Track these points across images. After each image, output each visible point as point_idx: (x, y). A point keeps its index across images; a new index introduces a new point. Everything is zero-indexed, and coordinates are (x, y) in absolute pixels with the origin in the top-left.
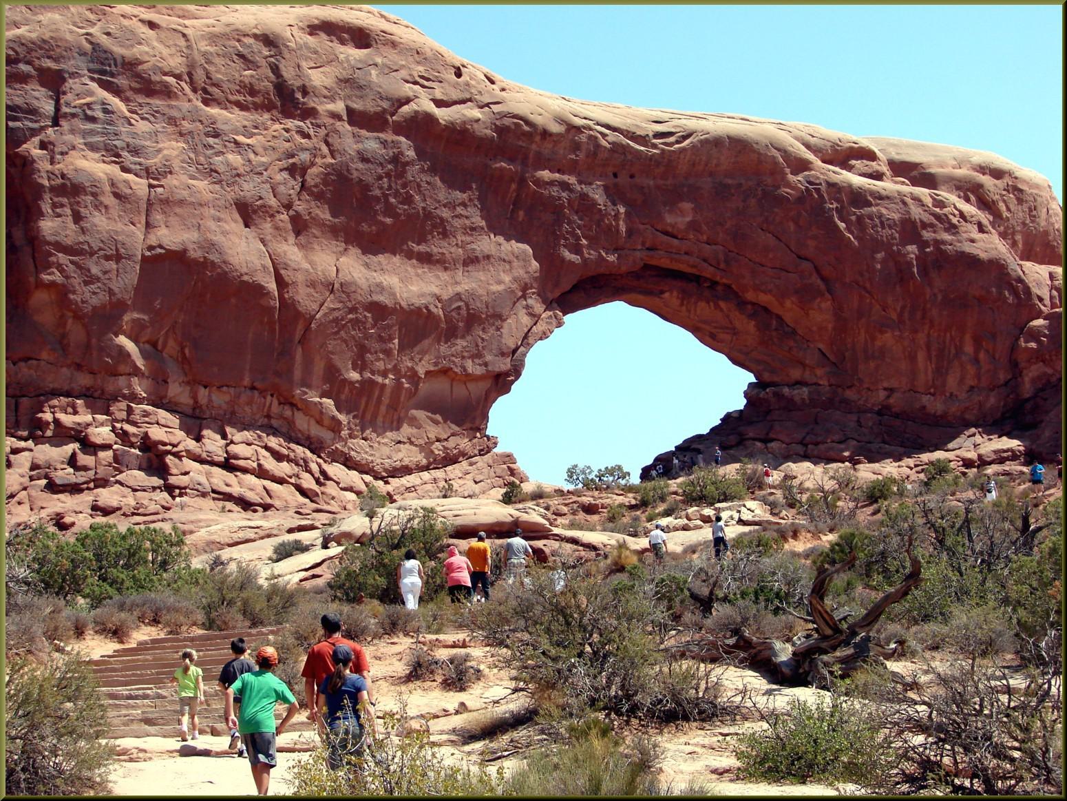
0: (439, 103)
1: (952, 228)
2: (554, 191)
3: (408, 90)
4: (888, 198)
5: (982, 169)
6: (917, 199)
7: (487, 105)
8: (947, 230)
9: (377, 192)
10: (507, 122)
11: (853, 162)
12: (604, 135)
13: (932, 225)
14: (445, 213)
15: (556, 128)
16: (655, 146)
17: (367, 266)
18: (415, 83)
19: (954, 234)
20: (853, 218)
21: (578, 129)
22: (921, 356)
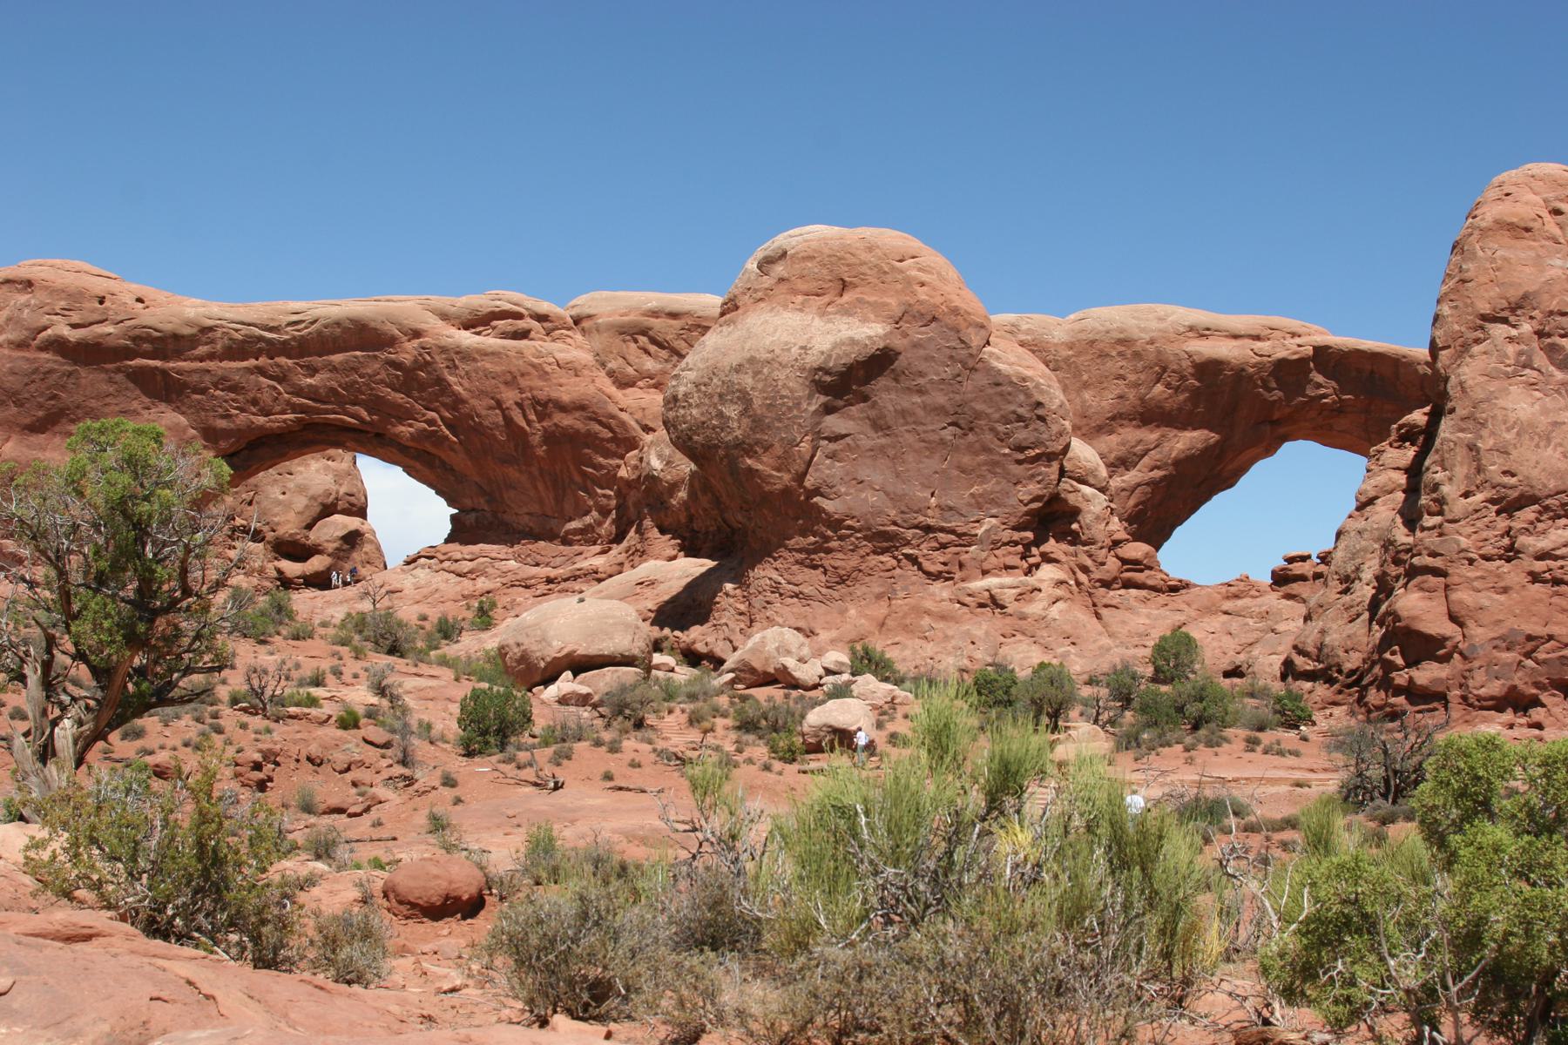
0: (74, 326)
1: (544, 375)
2: (195, 378)
3: (45, 320)
4: (493, 354)
5: (655, 314)
6: (520, 353)
7: (122, 321)
8: (540, 377)
9: (26, 395)
10: (137, 332)
11: (495, 323)
12: (237, 330)
13: (528, 374)
14: (93, 403)
15: (187, 331)
16: (287, 333)
17: (28, 446)
18: (57, 314)
19: (546, 380)
20: (463, 373)
21: (211, 329)
22: (540, 486)
